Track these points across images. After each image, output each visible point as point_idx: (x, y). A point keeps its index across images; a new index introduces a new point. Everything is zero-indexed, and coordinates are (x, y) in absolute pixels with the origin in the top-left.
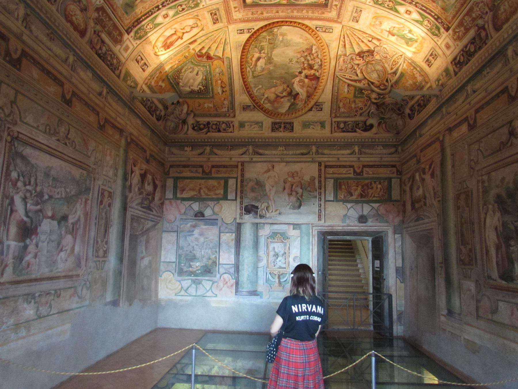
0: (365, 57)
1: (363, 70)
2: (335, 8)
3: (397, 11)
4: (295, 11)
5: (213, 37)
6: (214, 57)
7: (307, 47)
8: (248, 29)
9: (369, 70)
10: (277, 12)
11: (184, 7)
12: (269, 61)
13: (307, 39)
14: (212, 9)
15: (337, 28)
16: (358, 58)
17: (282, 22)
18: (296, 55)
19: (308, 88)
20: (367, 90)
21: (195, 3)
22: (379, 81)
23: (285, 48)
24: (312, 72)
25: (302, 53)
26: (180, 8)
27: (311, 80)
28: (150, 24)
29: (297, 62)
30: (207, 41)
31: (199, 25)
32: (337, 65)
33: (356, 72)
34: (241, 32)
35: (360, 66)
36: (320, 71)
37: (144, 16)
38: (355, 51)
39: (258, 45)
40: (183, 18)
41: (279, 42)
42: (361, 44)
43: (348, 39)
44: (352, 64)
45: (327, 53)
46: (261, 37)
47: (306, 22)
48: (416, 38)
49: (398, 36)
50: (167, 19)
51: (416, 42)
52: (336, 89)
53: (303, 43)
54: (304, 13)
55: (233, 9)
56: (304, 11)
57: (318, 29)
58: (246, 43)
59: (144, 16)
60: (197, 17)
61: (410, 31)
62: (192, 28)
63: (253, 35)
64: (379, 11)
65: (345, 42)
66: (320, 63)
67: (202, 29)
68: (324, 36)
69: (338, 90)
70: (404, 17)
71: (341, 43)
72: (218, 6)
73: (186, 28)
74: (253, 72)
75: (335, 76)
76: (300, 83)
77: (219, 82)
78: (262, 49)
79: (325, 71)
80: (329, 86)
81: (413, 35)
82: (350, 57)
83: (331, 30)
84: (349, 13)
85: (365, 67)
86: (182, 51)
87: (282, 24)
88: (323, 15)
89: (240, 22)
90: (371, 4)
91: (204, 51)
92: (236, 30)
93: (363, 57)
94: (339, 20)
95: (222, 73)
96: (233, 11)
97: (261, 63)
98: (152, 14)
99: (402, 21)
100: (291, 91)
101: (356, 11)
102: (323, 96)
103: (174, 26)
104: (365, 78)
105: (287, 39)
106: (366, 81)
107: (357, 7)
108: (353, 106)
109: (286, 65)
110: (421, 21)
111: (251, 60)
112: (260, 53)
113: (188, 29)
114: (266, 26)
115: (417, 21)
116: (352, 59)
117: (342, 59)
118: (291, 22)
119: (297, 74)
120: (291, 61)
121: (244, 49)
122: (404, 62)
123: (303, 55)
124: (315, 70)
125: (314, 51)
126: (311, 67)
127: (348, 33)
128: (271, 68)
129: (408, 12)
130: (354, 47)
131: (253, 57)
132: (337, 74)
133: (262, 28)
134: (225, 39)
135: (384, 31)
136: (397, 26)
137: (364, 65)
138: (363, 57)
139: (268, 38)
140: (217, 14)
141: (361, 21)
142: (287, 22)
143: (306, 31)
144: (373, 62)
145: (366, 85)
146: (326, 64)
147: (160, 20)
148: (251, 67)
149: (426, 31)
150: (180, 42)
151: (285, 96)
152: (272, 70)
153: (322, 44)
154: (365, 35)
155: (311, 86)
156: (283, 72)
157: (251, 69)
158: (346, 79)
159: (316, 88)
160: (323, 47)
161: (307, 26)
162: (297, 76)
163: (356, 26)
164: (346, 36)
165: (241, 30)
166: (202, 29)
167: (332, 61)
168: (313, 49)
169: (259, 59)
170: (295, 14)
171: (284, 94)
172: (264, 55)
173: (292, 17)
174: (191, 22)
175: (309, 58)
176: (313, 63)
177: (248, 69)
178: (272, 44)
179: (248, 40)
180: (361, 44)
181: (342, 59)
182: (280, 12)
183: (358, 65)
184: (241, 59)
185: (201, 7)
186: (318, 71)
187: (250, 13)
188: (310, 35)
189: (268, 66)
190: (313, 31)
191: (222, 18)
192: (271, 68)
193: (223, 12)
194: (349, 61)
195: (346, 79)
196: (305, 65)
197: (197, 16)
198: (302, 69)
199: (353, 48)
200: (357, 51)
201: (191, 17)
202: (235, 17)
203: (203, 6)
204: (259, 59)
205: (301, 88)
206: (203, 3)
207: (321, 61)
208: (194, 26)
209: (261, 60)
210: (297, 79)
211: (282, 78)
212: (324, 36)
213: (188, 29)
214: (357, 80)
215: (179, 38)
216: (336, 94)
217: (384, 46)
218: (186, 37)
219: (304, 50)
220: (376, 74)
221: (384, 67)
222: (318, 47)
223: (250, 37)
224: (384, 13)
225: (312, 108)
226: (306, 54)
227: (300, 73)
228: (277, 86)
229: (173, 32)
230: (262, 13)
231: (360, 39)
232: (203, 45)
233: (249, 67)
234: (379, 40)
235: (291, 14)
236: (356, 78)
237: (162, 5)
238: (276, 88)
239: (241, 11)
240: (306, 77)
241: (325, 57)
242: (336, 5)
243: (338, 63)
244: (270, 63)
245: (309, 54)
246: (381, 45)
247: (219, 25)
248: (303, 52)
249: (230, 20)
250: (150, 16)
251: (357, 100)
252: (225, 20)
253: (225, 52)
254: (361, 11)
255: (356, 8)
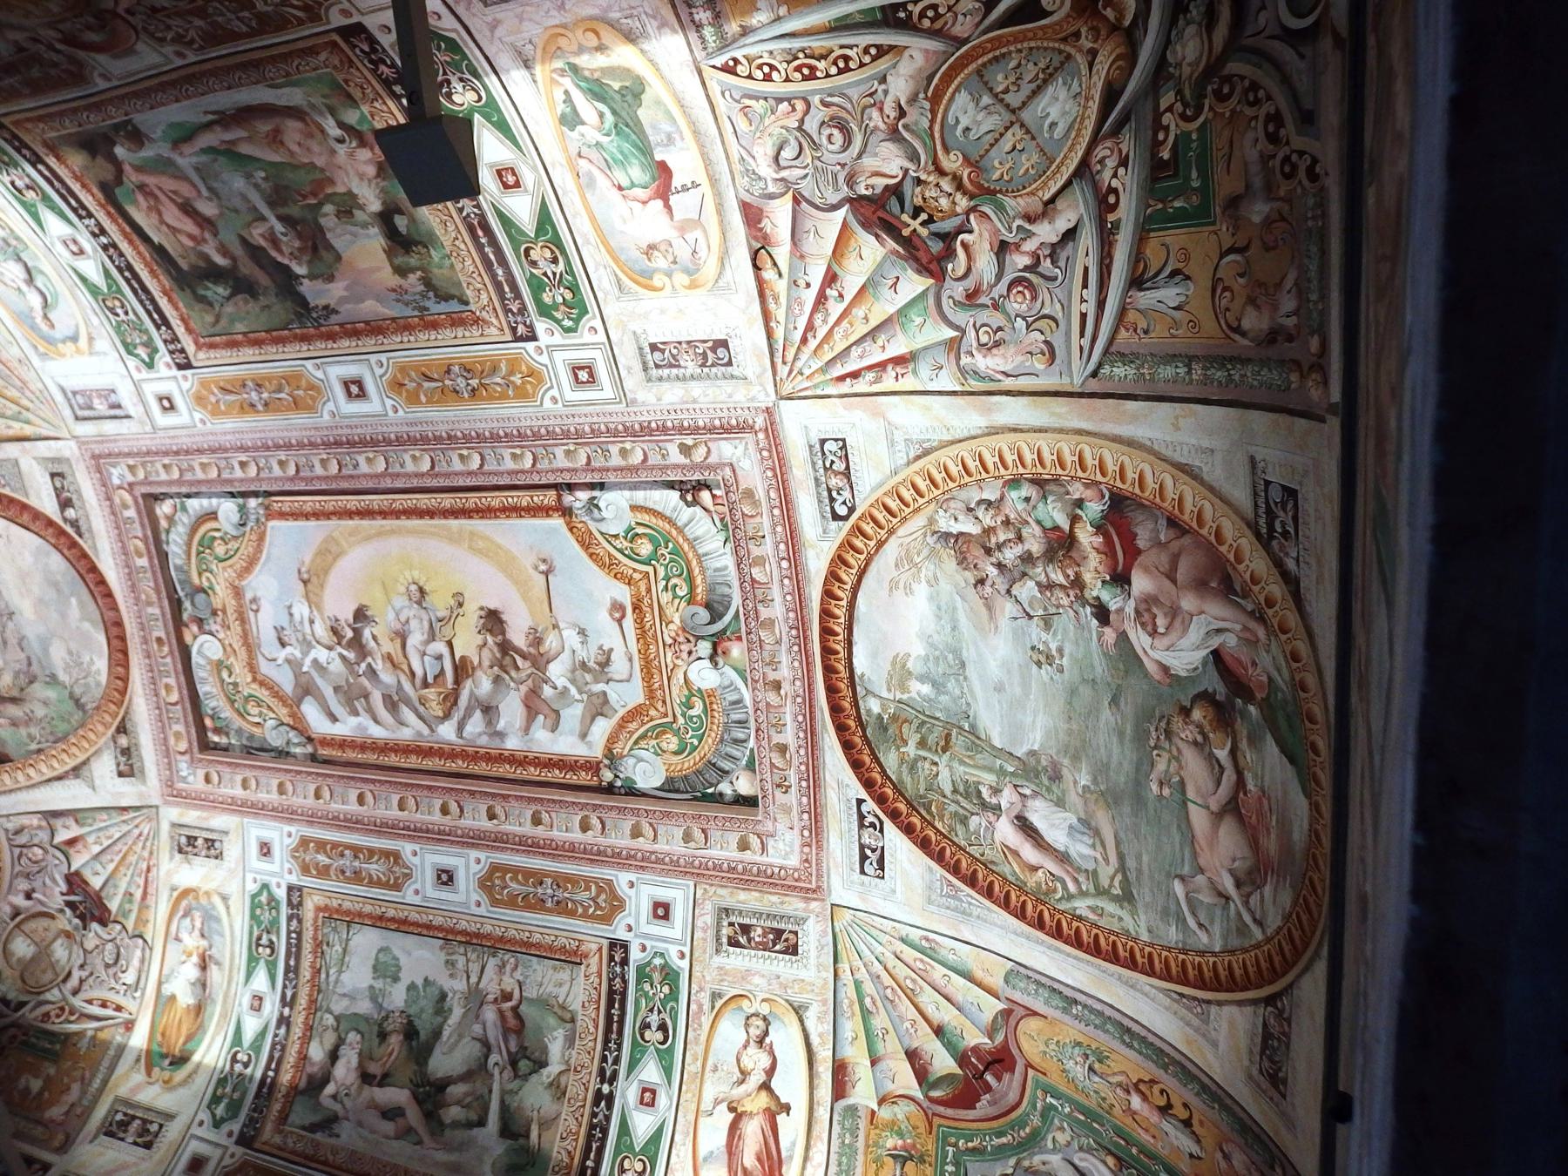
0: (947, 226)
1: (1034, 204)
2: (702, 450)
3: (544, 219)
4: (765, 613)
5: (869, 987)
6: (1000, 1038)
7: (951, 564)
8: (861, 826)
9: (1028, 161)
10: (777, 686)
11: (654, 1019)
12: (1038, 773)
13: (906, 560)
14: (711, 933)
15: (803, 424)
16: (959, 264)
17: (829, 670)
18: (1004, 623)
19: (1182, 574)
20: (1158, 126)
21: (656, 977)
22: (1093, 53)
23: (971, 671)
24: (1087, 537)
25: (988, 589)
26: (654, 1036)
27: (1133, 553)
28: (626, 1164)
29: (1047, 623)
30: (880, 1021)
31: (765, 1009)
32: (1024, 383)
33: (1054, 250)
34: (872, 860)
35: (1010, 237)
36: (1077, 491)
37: (586, 1157)
38: (924, 294)
39: (953, 808)
40: (696, 1049)
41: (942, 698)
42: (852, 282)
43: (855, 352)
44: (1002, 287)
45: (964, 451)
46: (907, 779)
47: (817, 563)
48: (567, 82)
49: (645, 150)
50: (662, 1100)
51: (575, 69)
52: (1167, 372)
53: (933, 582)
54: (770, 573)
55: (748, 856)
56: (757, 573)
57: (842, 511)
58: (939, 858)
59: (586, 1157)
60: (722, 1003)
61: (571, 120)
62: (761, 1042)
63: (894, 815)
64: (603, 279)
65: (882, 365)
66: (1027, 490)
67: (799, 1011)
68: (872, 478)
69: (1170, 358)
70: (539, 183)
71: (888, 383)
72: (708, 906)
73: (747, 1063)
74: (1100, 892)
75: (1093, 386)
76: (1161, 623)
77: (1136, 1102)
78: (970, 791)
79: (1069, 458)
80: (1154, 424)
81: (568, 99)
82: (961, 317)
83: (829, 446)
84: (696, 389)
85: (1008, 201)
86: (849, 1151)
87: (844, 674)
88: (760, 493)
89: (819, 847)
90: (598, 323)
91: (943, 1063)
92: (857, 875)
93: (948, 238)
94: (760, 422)
95: (1096, 1059)
96: (758, 858)
97: (1053, 824)
98: (605, 1131)
99: (563, 178)
100: (1205, 697)
101: (671, 366)
102: (1214, 472)
103: (709, 1093)
104: (1083, 170)
105: (926, 659)
106: (1100, 152)
107: (645, 369)
108: (1258, 211)
109: (1073, 692)
110: (487, 117)
111: (1035, 869)
112: (997, 809)
113: (757, 1060)
114: (847, 746)
115: (503, 127)
116: (972, 296)
117: (983, 362)
118: (826, 632)
119: (1110, 635)
120: (1049, 659)
121: (971, 881)
122: (745, 31)
123: (1003, 588)
124: (1075, 519)
125: (972, 528)
126: (1061, 545)
127: (817, 364)
128: (1084, 780)
129: (511, 180)
130: (892, 310)
131: (1016, 853)
132: (1077, 377)
133: (856, 765)
134: (902, 940)
135: (678, 215)
136: (602, 181)
137: (1000, 208)
138: (948, 238)
139: (911, 749)
140: (747, 921)
141: (706, 328)
142: (827, 651)
143: (868, 563)
144: (951, 162)
145: (1127, 144)
146: (1029, 457)
147: (643, 1124)
148: (1072, 887)
149: (492, 81)
150: (791, 1129)
151: (1233, 753)
152: (1095, 781)
153: (922, 485)
154: (781, 286)
155: (1164, 560)
156: (1106, 715)
157: (1083, 894)
158: (1101, 304)
159: (1172, 522)
160: (938, 477)
161: (839, 560)
162: (1123, 637)
163: (749, 343)
164: (839, 371)
165: (863, 858)
166: (799, 1011)
167: (1002, 419)
168: (955, 528)
169: (1025, 826)
170: (777, 610)
171: (1222, 754)
172: (1007, 798)
173: (801, 625)
174: (731, 1032)
175: (1010, 555)
176: (1037, 530)
177: (1082, 906)
178: (948, 736)
179: (924, 845)
180: (852, 282)
181: (983, 362)
182: (772, 676)
183: (1002, 249)
184: (1021, 914)
185: (685, 964)
186: (1079, 503)
187: (778, 793)
188: (881, 544)
189: (1073, 798)
190: (858, 530)
191: (774, 910)
192: (1084, 780)
193: (748, 900)
194: (984, 316)
195: (1101, 304)
196: (1059, 578)
197: (715, 996)
198: (1083, 601)
199: (902, 312)
200: (914, 284)
201: (706, 1021)
202: (794, 861)
203: (682, 956)
204: (1025, 826)
205: (1185, 630)
206: (673, 951)
207: (1014, 483)
208: (755, 1032)
209: (1036, 819)
210: (1140, 639)
211: (1140, 737)
212: (872, 478)
213: (757, 1060)
214: (1101, 222)
215: (771, 1116)
216: (1197, 372)
217: (766, 170)
218: (791, 1085)
219: (970, 577)
220: (1043, 102)
221: (933, 90)
222: (943, 503)
223: (908, 830)
224: (594, 256)
225: (1285, 575)
226: (992, 571)
227: (1102, 614)
228: (1182, 783)
229: (724, 1118)
230: (783, 749)
231: (821, 299)
232: (892, 1048)
233: (1070, 897)
234: (752, 216)
235: (782, 629)
236: (1088, 239)
237: (602, 1082)
238: (1191, 794)
239: (769, 826)
240: (1120, 579)
241: (990, 461)
242: (685, 450)
243: (1008, 383)
244: (1056, 777)
245: (988, 551)
246: (772, 188)
247: (813, 936)
248: (981, 582)
249: (806, 883)
250: (603, 1140)
251: (1226, 185)
252: (794, 905)
253: (979, 974)
254: (654, 347)
255: (654, 372)
